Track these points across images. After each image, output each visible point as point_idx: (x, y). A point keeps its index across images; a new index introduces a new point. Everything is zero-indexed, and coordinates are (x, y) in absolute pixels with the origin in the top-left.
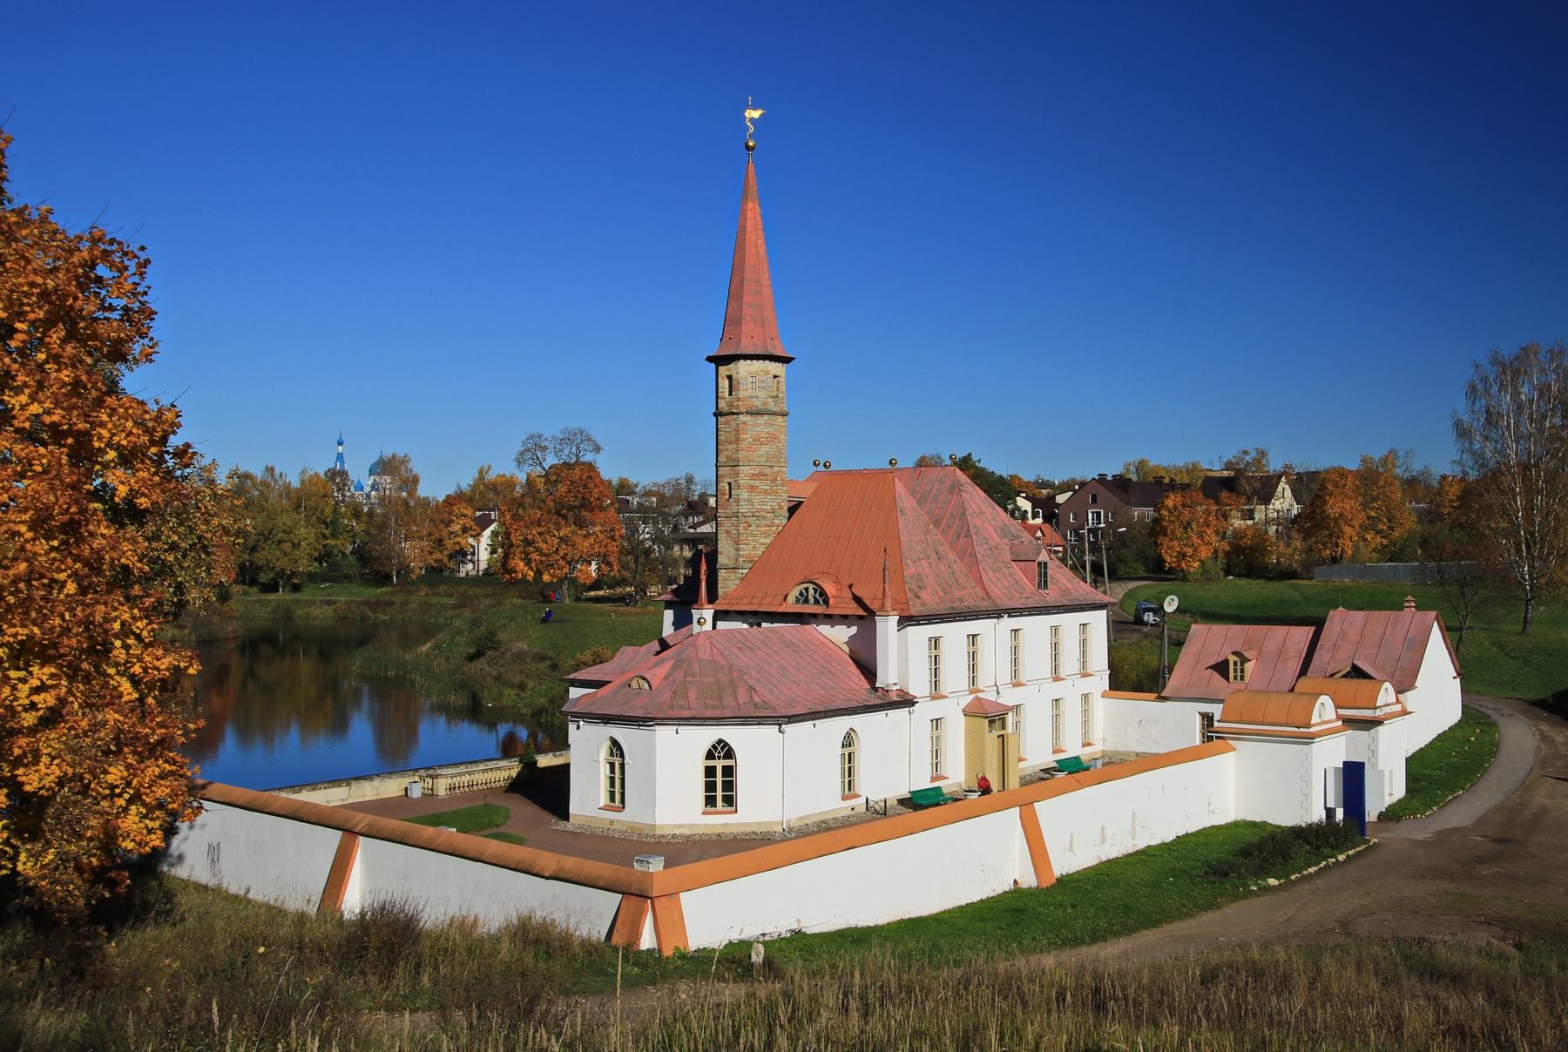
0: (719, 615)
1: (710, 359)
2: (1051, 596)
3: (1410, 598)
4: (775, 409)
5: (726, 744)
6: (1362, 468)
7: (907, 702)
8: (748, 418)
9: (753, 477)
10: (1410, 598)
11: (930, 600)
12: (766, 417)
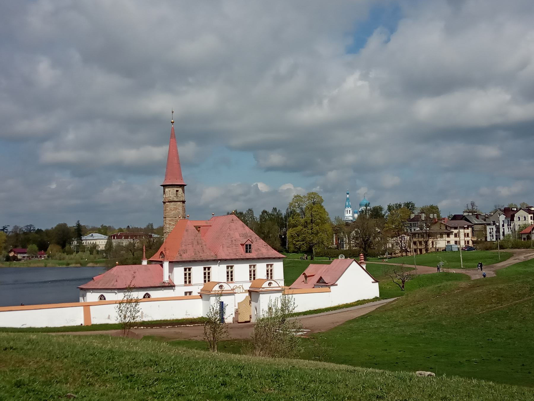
0: (150, 262)
1: (161, 186)
2: (248, 255)
3: (361, 254)
4: (177, 200)
5: (104, 297)
6: (52, 230)
7: (171, 286)
8: (169, 203)
9: (170, 221)
10: (361, 254)
11: (185, 257)
12: (173, 203)
